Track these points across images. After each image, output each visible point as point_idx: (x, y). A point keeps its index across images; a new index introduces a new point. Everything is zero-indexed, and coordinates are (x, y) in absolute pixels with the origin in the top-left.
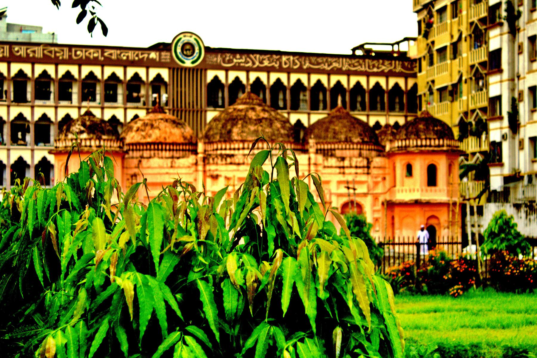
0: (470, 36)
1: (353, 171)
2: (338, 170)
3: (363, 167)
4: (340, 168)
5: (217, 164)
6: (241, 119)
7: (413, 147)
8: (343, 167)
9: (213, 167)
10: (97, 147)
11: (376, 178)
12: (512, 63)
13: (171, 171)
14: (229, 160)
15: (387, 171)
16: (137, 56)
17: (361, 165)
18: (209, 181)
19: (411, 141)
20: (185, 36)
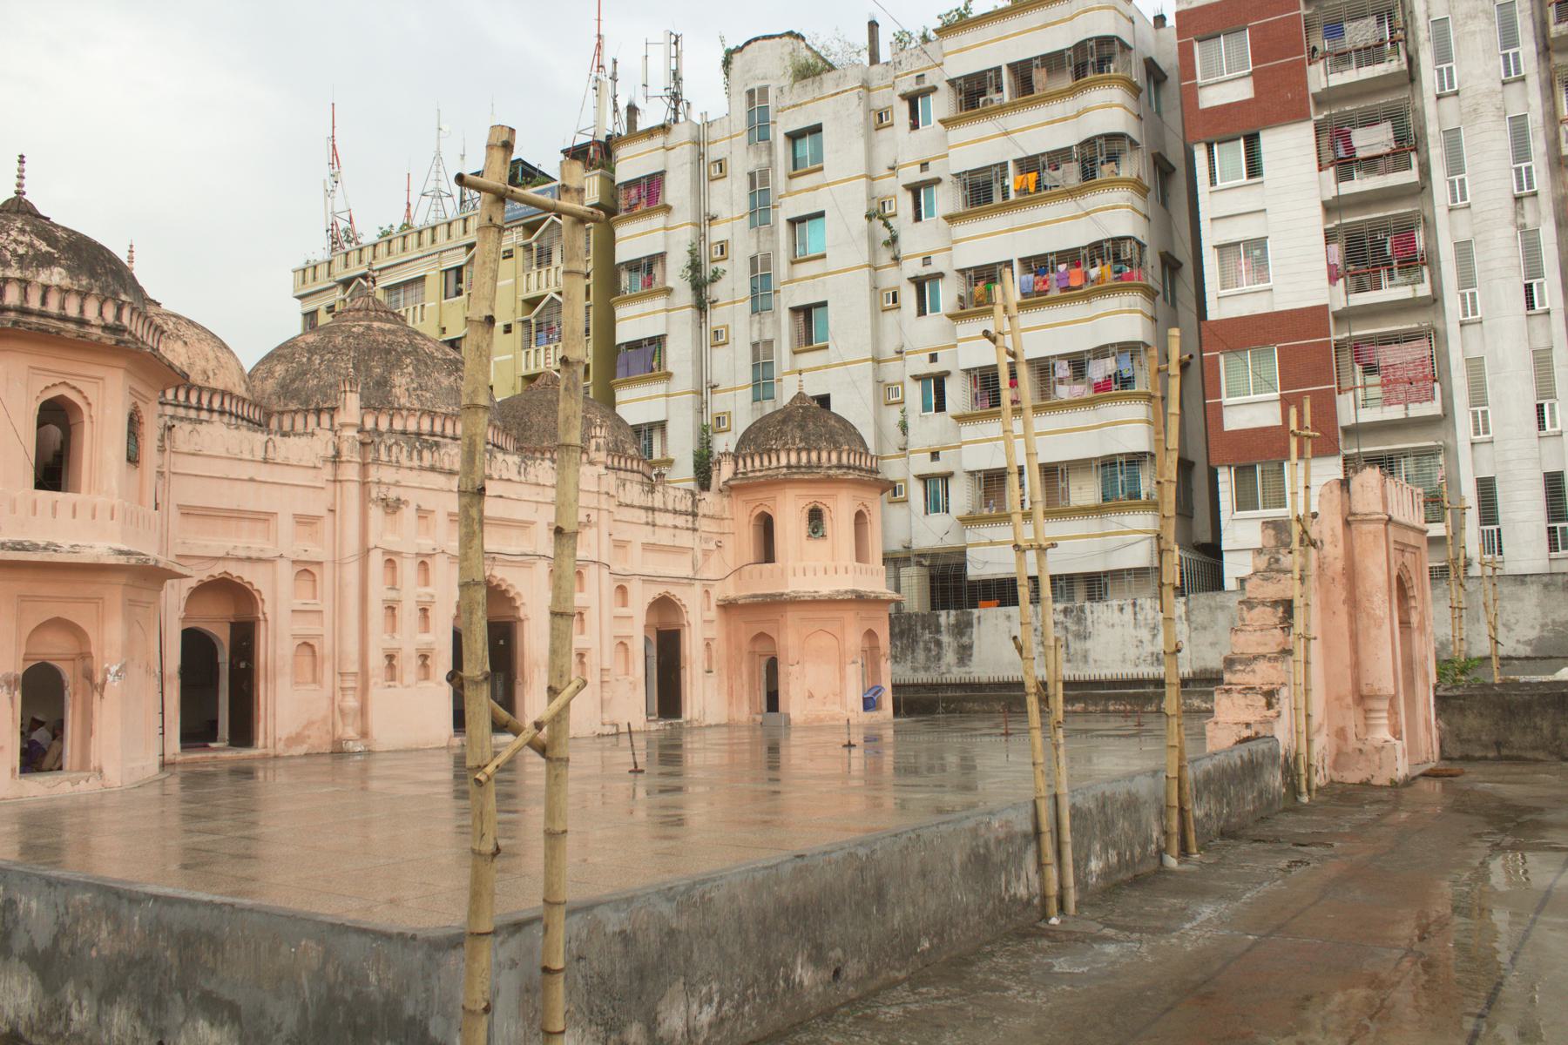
0: (526, 323)
1: (669, 519)
2: (642, 516)
3: (686, 513)
4: (647, 509)
5: (398, 465)
6: (407, 353)
7: (829, 468)
8: (653, 509)
9: (387, 474)
10: (106, 328)
11: (707, 541)
12: (700, 363)
13: (264, 473)
14: (426, 454)
15: (727, 526)
17: (683, 508)
18: (376, 513)
19: (824, 455)
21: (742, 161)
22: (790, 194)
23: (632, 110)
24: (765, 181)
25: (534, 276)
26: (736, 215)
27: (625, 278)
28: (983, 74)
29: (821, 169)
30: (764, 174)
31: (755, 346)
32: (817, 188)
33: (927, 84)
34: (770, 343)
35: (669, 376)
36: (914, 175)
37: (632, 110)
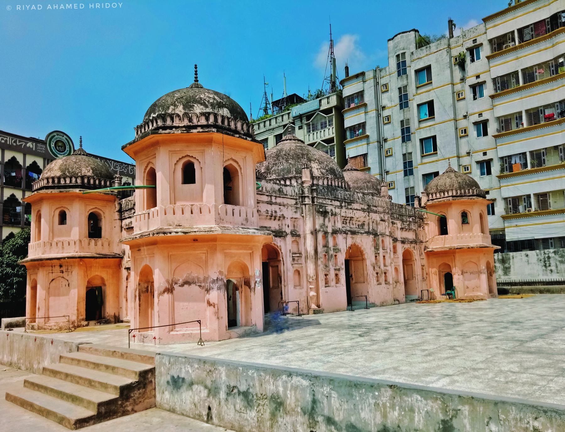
5: (325, 199)
16: (15, 142)
20: (58, 135)
21: (395, 83)
22: (417, 94)
23: (347, 68)
24: (406, 90)
25: (311, 135)
26: (393, 105)
27: (348, 134)
28: (505, 35)
29: (431, 83)
30: (405, 87)
31: (404, 155)
32: (430, 91)
33: (478, 43)
34: (411, 153)
35: (369, 169)
36: (474, 81)
37: (347, 68)
